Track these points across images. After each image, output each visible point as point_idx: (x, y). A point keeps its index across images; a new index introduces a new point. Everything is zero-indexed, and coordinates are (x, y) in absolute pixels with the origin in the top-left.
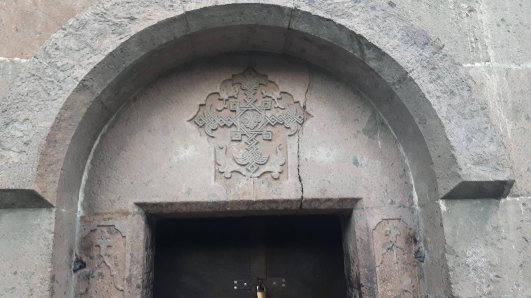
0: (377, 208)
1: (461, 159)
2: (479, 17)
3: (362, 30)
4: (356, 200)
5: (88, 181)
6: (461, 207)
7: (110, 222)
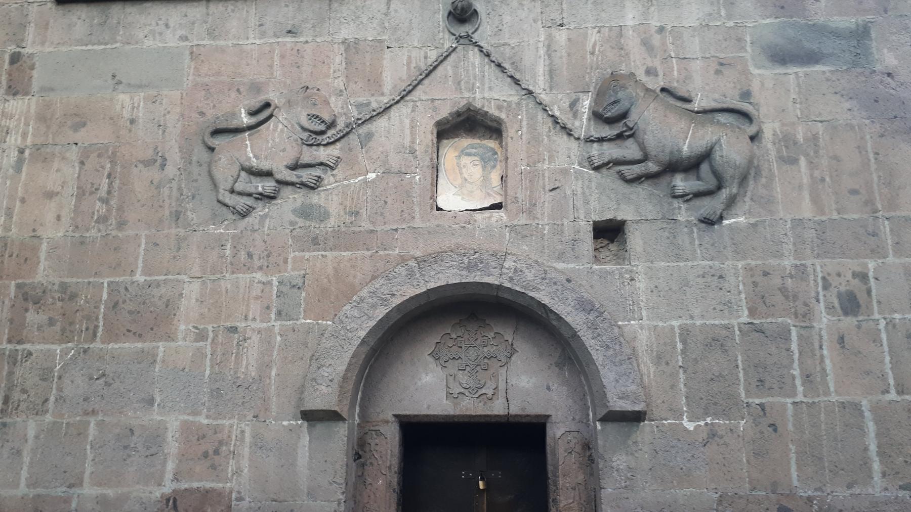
0: (564, 422)
1: (610, 395)
2: (638, 285)
3: (546, 300)
4: (548, 416)
5: (362, 399)
6: (611, 427)
7: (377, 428)
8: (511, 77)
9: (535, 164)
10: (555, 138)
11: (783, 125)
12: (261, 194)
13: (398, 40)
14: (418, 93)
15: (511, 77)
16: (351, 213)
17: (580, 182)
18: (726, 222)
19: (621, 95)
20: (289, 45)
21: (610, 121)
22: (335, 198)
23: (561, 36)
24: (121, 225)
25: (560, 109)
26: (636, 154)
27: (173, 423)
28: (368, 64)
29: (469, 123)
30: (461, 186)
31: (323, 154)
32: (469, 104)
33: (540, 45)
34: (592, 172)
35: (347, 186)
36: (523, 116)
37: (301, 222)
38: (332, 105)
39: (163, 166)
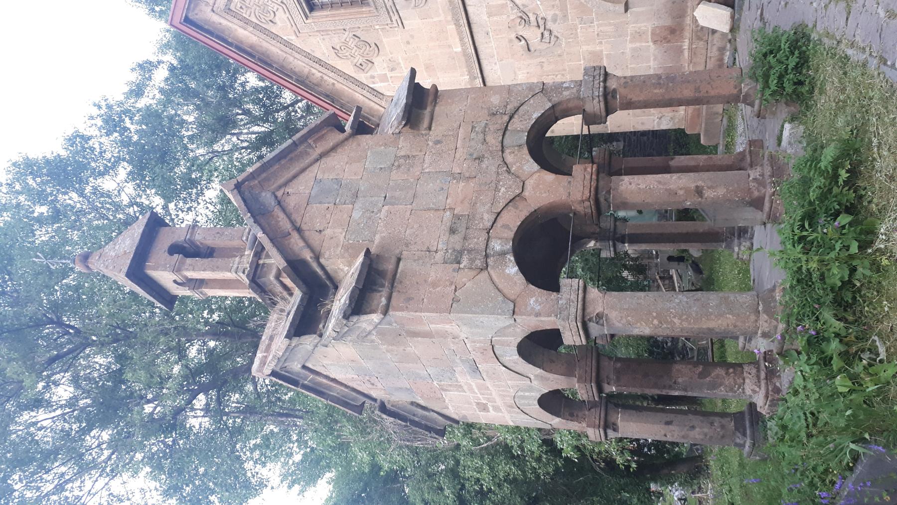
24: (565, 70)
27: (630, 46)
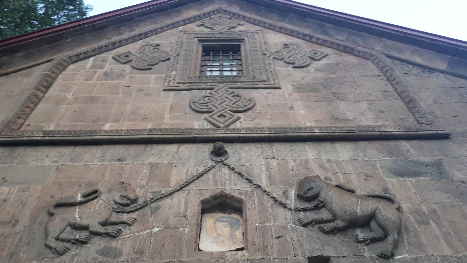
8: (247, 179)
9: (265, 223)
10: (276, 209)
11: (413, 205)
12: (77, 240)
13: (182, 163)
14: (192, 186)
15: (247, 179)
16: (137, 253)
17: (295, 234)
18: (396, 258)
19: (313, 185)
20: (117, 165)
21: (309, 200)
22: (128, 243)
23: (274, 163)
25: (277, 194)
26: (330, 216)
28: (163, 173)
29: (222, 204)
30: (216, 238)
31: (125, 217)
32: (223, 192)
33: (263, 166)
34: (302, 228)
35: (138, 235)
36: (255, 197)
37: (100, 258)
38: (137, 192)
39: (14, 226)
